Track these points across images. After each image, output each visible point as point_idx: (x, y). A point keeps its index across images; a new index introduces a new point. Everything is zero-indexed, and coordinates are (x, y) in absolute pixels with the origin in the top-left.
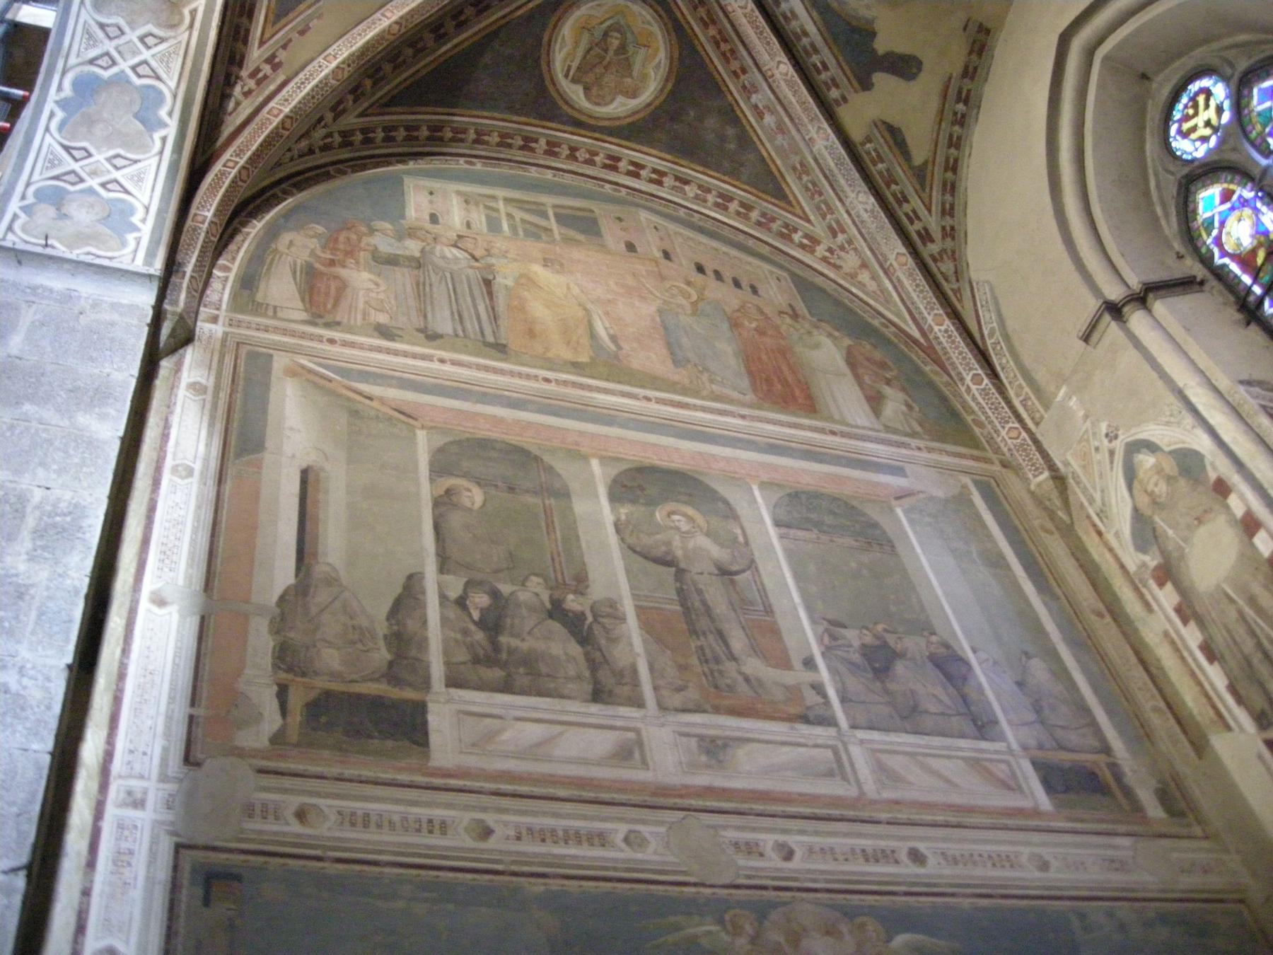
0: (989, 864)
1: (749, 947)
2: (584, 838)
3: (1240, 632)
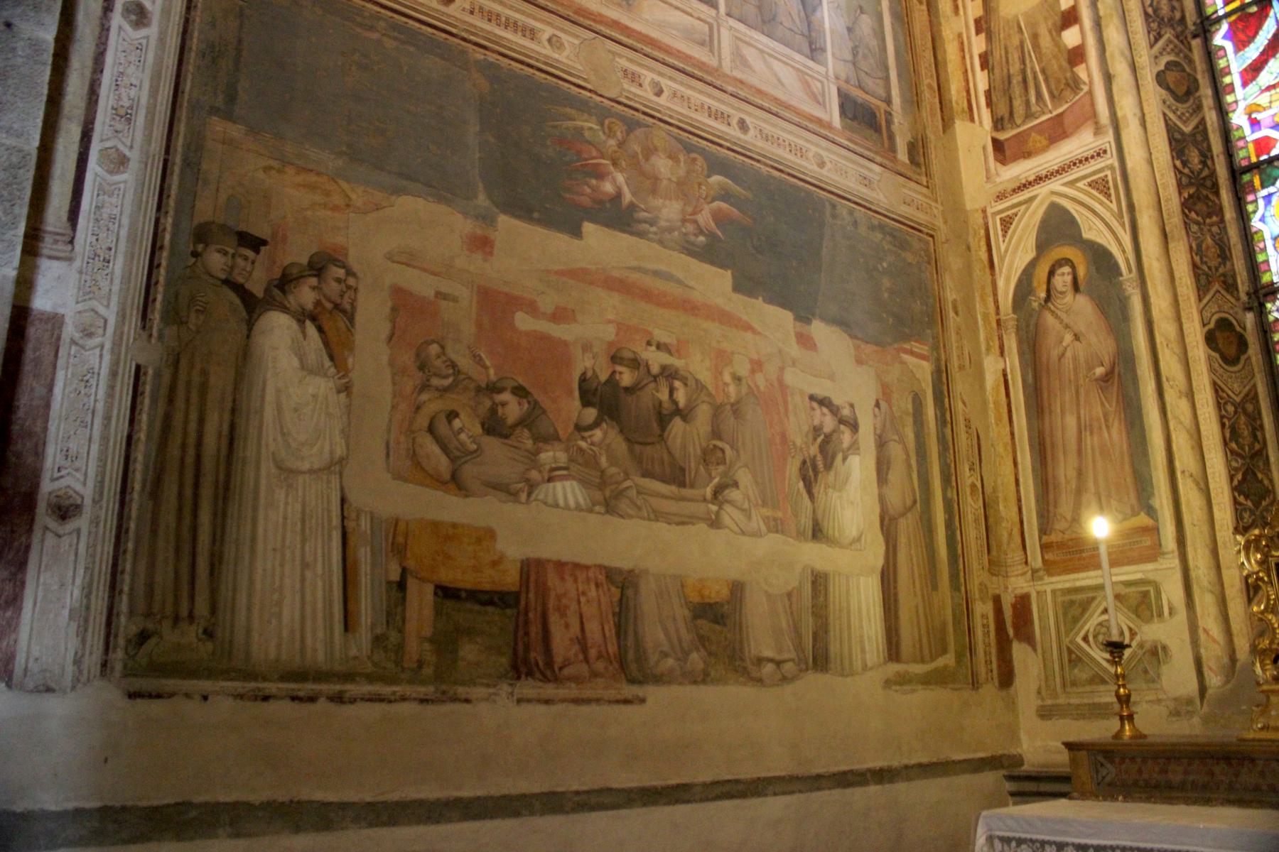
0: (788, 149)
1: (616, 148)
2: (520, 29)
3: (1014, 56)
